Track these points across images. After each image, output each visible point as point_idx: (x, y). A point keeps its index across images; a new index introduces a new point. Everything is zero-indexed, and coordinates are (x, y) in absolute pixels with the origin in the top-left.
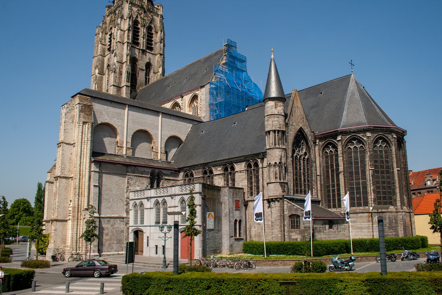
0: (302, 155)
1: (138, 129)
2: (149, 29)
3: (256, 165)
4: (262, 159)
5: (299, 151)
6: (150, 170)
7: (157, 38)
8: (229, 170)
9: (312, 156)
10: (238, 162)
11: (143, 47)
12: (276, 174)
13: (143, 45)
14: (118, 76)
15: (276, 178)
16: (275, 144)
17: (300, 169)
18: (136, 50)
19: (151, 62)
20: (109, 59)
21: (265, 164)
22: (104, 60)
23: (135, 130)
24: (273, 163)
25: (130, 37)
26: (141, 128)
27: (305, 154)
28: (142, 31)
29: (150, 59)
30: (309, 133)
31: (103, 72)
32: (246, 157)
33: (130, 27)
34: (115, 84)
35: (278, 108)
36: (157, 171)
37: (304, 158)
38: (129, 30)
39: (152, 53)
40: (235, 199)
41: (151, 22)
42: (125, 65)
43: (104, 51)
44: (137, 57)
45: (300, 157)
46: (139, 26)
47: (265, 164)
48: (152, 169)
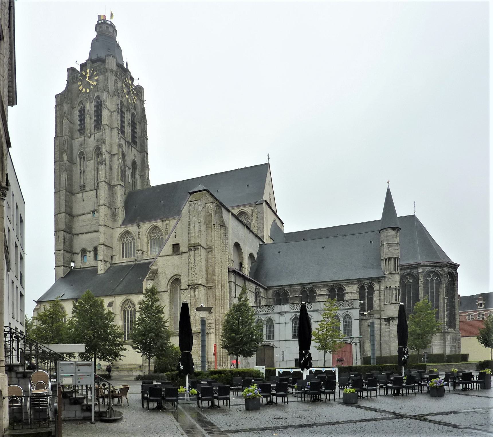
3: (371, 287)
4: (379, 282)
8: (336, 291)
10: (348, 284)
12: (396, 296)
15: (396, 300)
16: (395, 270)
20: (81, 145)
21: (383, 287)
22: (72, 143)
24: (393, 286)
31: (72, 160)
32: (359, 280)
42: (116, 157)
43: (71, 131)
46: (124, 110)
47: (383, 287)
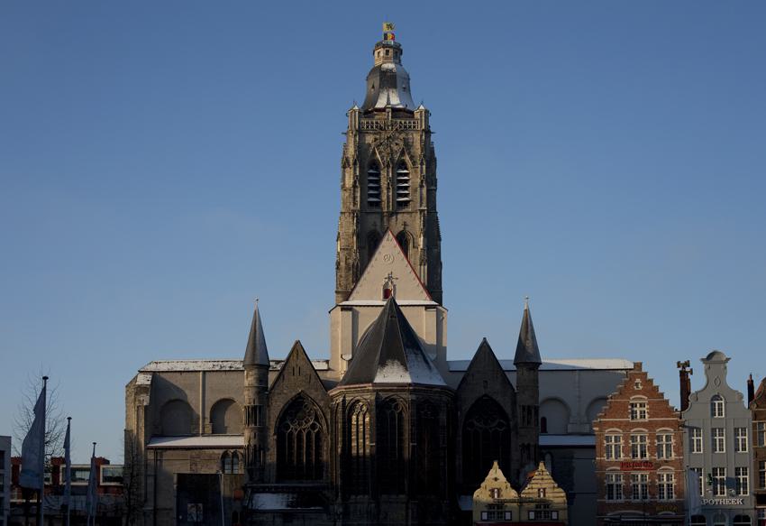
0: (304, 429)
1: (219, 398)
2: (403, 165)
5: (300, 424)
6: (221, 451)
7: (415, 178)
9: (325, 427)
11: (388, 207)
13: (388, 202)
14: (343, 274)
17: (300, 447)
18: (374, 216)
19: (408, 229)
23: (214, 401)
25: (358, 199)
26: (222, 397)
27: (313, 426)
28: (385, 177)
29: (405, 224)
30: (320, 397)
33: (355, 182)
34: (340, 290)
35: (249, 379)
36: (232, 451)
37: (309, 434)
38: (354, 186)
39: (408, 213)
40: (235, 487)
41: (403, 153)
44: (379, 229)
45: (300, 431)
48: (224, 450)
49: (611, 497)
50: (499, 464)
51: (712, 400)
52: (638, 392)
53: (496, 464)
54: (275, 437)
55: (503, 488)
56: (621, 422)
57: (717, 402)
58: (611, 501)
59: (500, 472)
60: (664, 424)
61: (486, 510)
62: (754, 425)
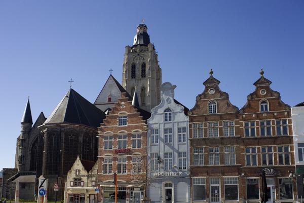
49: (105, 172)
50: (80, 157)
51: (165, 111)
52: (123, 110)
53: (78, 158)
54: (30, 152)
55: (81, 170)
56: (112, 127)
57: (168, 113)
58: (106, 174)
59: (80, 161)
60: (136, 127)
61: (72, 180)
62: (190, 126)
